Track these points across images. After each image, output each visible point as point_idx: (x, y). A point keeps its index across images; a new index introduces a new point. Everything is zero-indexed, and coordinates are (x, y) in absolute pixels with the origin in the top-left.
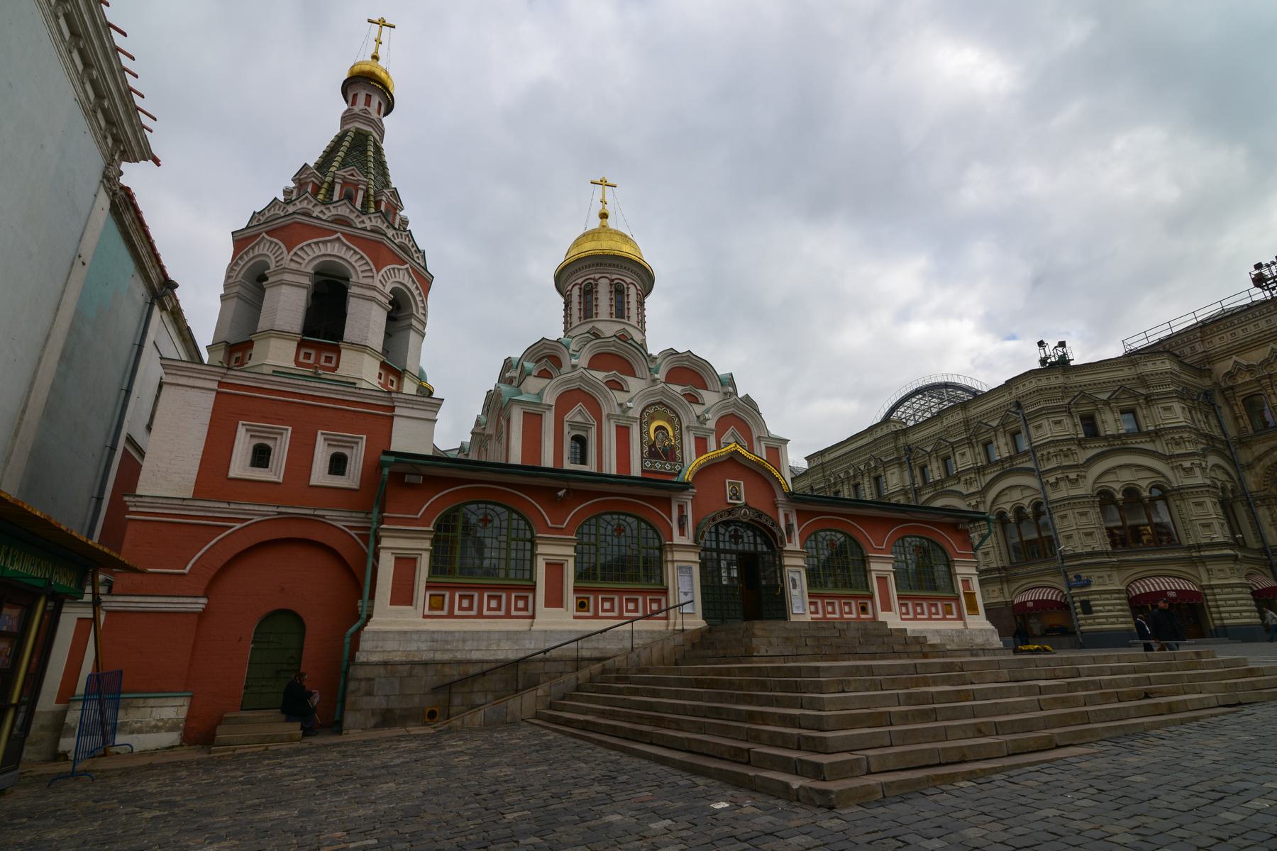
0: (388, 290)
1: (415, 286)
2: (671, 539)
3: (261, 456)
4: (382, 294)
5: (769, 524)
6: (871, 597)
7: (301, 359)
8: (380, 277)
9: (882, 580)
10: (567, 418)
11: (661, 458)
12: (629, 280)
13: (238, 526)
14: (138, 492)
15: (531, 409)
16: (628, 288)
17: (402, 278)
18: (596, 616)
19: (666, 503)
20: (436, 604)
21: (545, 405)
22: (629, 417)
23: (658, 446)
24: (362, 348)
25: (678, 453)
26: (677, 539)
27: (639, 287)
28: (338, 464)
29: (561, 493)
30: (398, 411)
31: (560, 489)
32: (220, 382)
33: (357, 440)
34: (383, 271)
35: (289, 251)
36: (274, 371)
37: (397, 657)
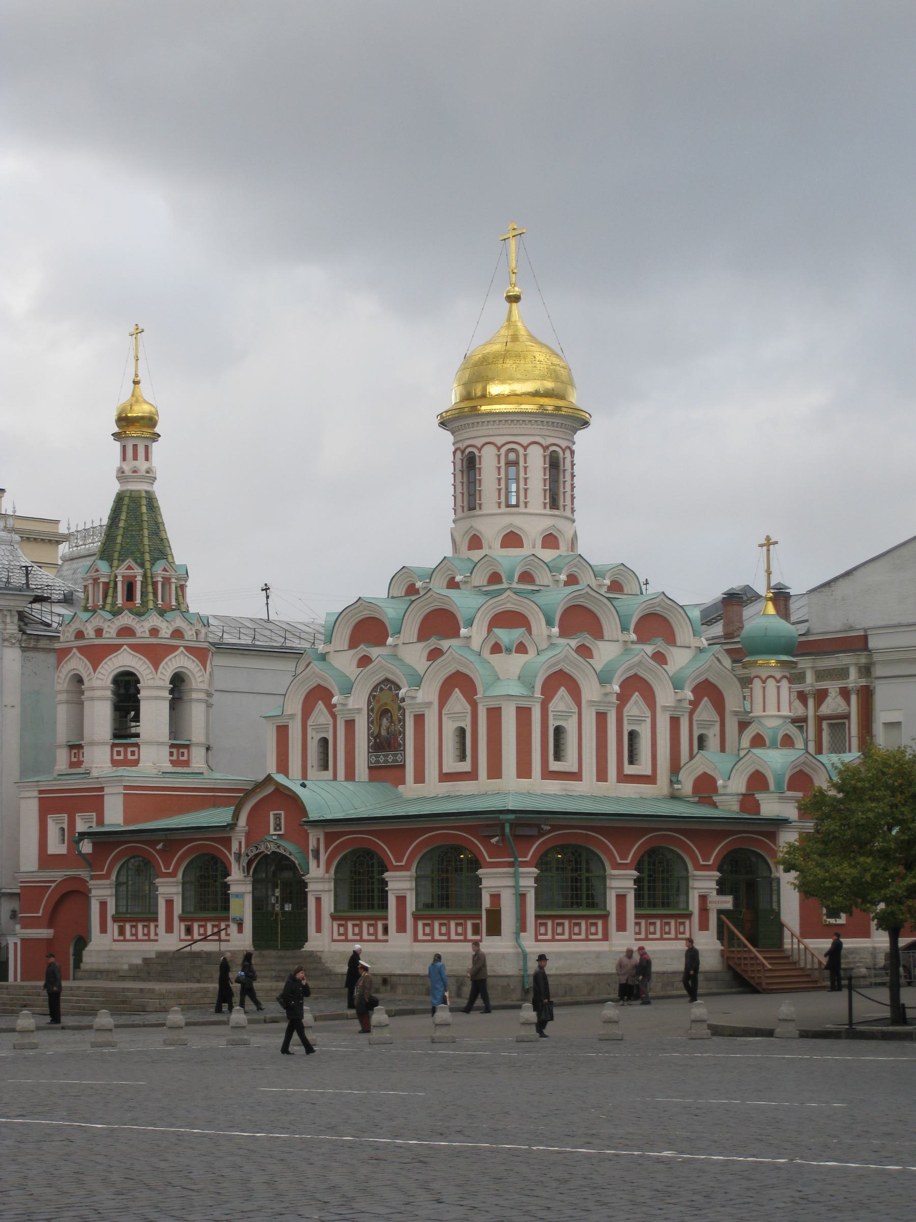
0: (108, 682)
1: (137, 659)
4: (102, 688)
5: (287, 855)
6: (386, 918)
10: (309, 723)
12: (479, 442)
13: (53, 885)
14: (22, 870)
15: (281, 722)
16: (480, 457)
17: (126, 660)
19: (227, 842)
20: (122, 932)
21: (287, 715)
22: (349, 710)
23: (383, 733)
24: (92, 744)
27: (499, 441)
29: (159, 847)
30: (107, 791)
31: (159, 842)
32: (39, 791)
33: (92, 817)
36: (59, 775)
37: (95, 967)
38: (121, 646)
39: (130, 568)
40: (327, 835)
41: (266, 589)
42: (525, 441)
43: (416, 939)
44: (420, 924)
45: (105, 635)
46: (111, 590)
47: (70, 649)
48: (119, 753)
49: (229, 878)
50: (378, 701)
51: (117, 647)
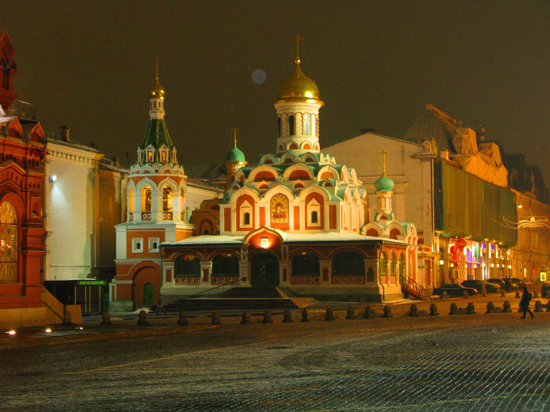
2: (240, 261)
3: (138, 246)
6: (319, 276)
7: (144, 218)
8: (159, 187)
9: (326, 270)
11: (279, 217)
13: (136, 264)
18: (219, 284)
20: (177, 281)
23: (278, 212)
25: (287, 214)
26: (242, 261)
28: (155, 245)
29: (204, 250)
34: (159, 185)
35: (135, 186)
38: (166, 177)
39: (164, 148)
40: (290, 248)
41: (127, 154)
42: (311, 113)
43: (332, 283)
44: (334, 277)
45: (160, 172)
46: (157, 156)
47: (144, 177)
48: (165, 216)
49: (239, 262)
50: (276, 201)
51: (166, 177)
